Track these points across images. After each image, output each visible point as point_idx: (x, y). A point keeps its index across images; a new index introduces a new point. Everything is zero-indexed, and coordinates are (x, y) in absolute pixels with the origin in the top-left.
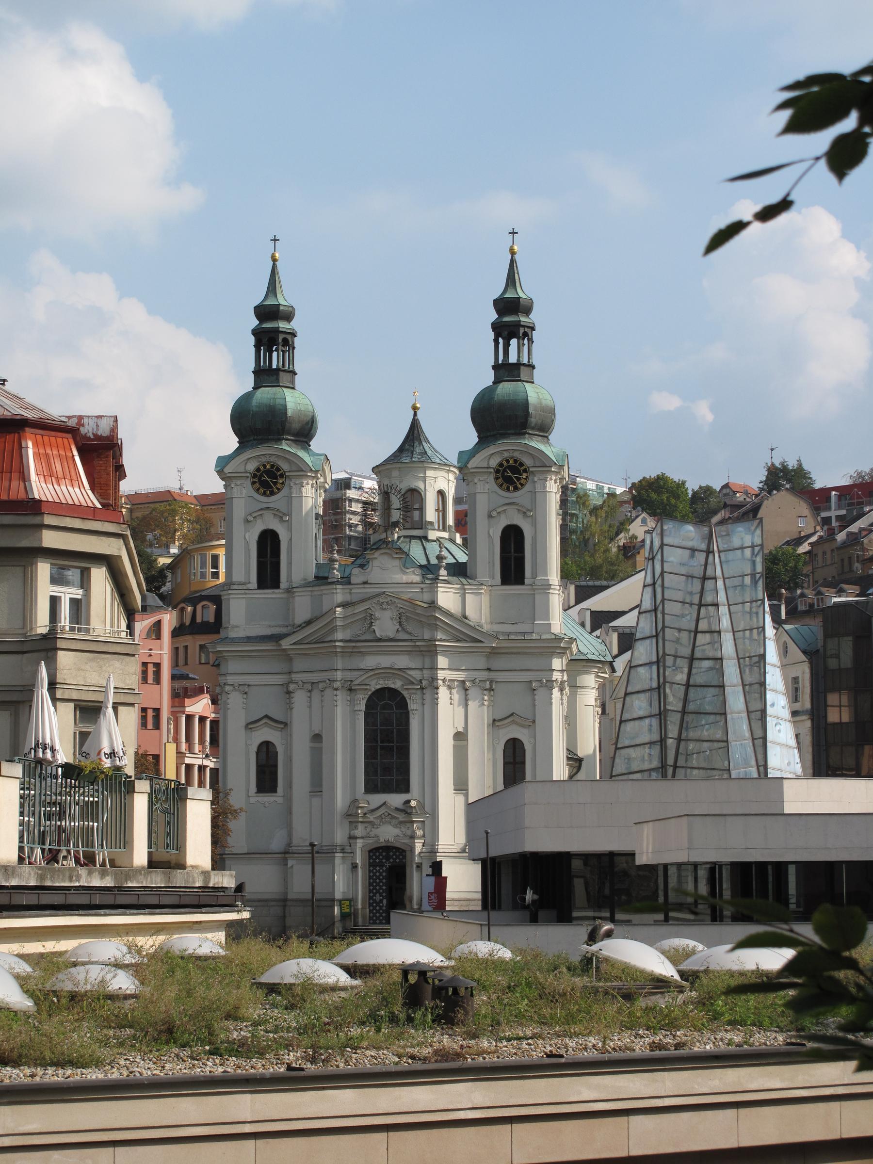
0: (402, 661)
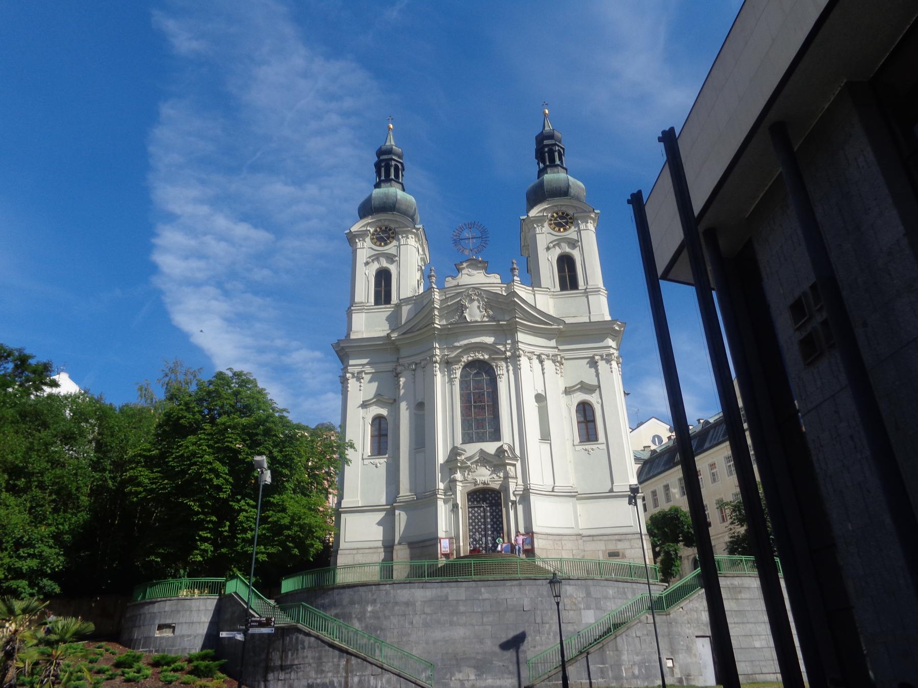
0: (490, 340)
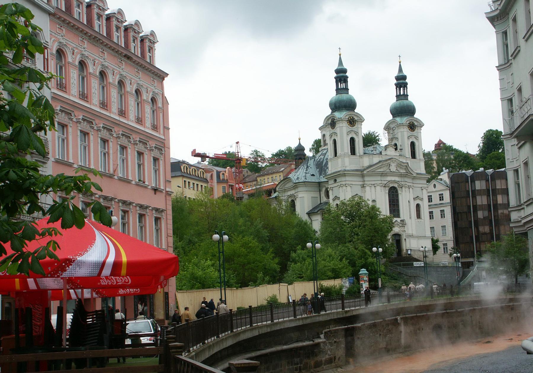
0: (397, 179)
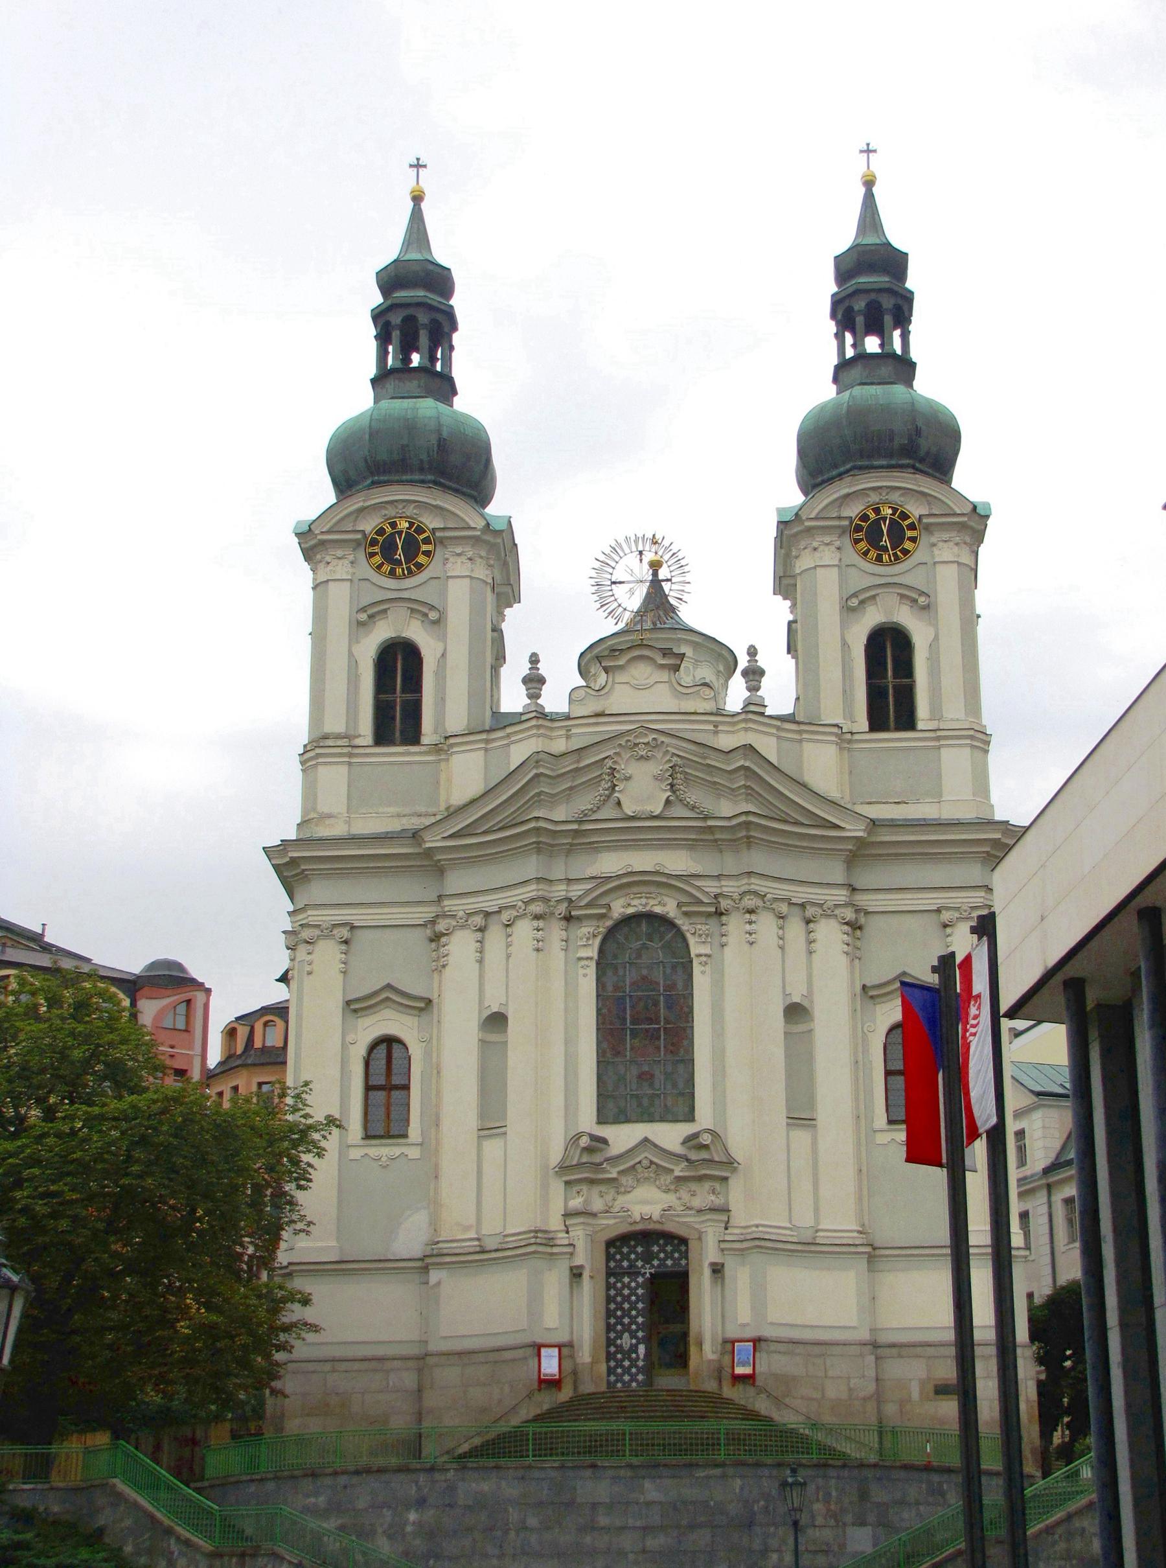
0: (677, 862)
